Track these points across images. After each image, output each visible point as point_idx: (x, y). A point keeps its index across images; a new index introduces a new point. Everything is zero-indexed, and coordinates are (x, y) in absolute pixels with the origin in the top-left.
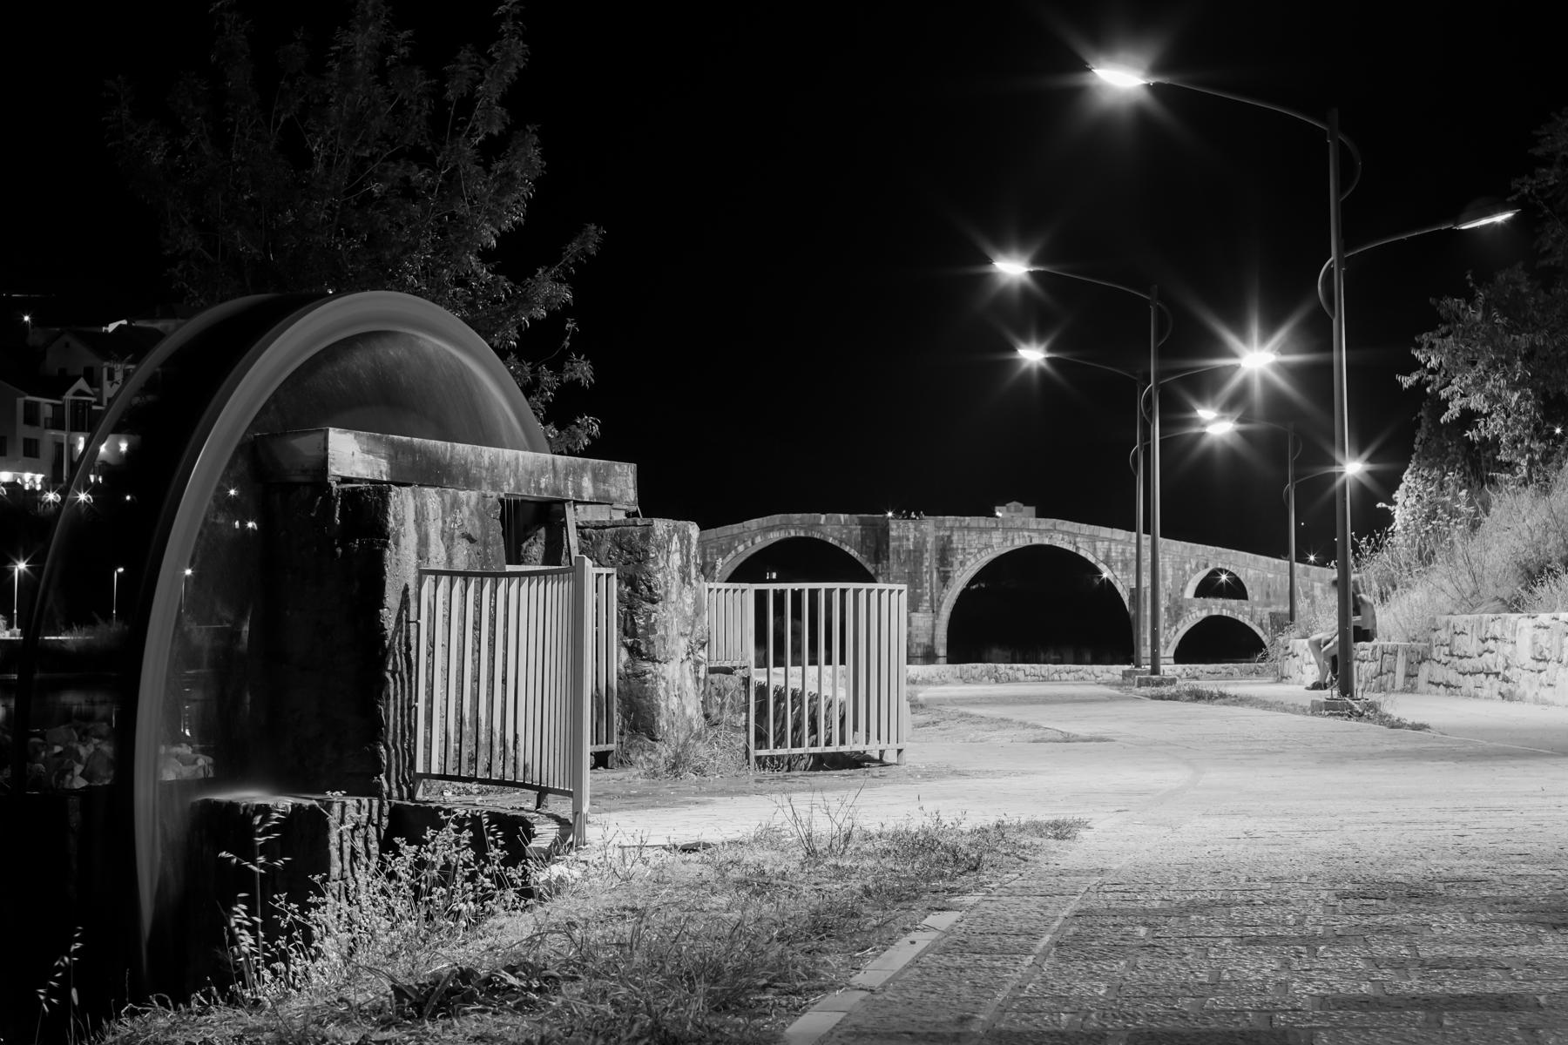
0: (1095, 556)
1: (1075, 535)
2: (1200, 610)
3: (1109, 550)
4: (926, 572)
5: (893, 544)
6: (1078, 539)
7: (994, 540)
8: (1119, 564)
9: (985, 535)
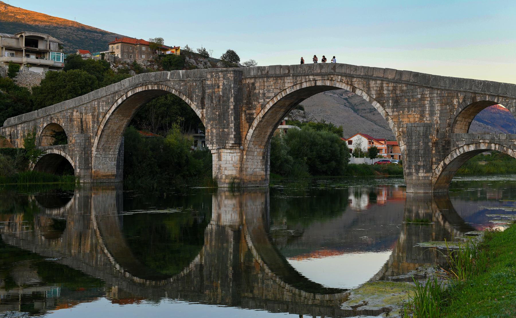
0: (368, 95)
1: (352, 77)
2: (468, 145)
3: (382, 88)
4: (232, 115)
5: (208, 91)
6: (355, 80)
7: (287, 85)
8: (391, 101)
9: (279, 81)
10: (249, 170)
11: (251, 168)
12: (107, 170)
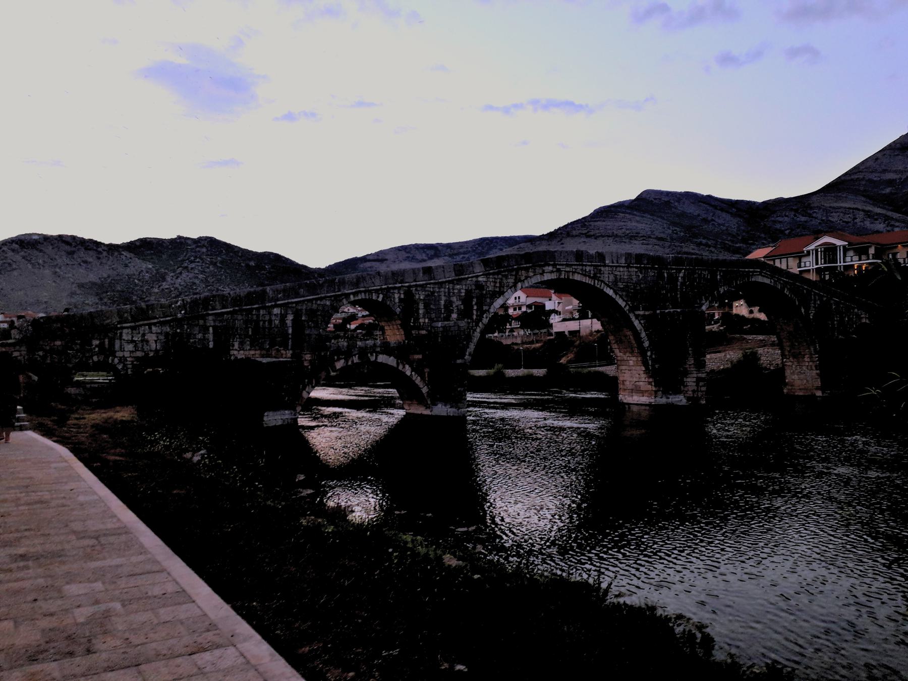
10: (627, 383)
11: (630, 381)
12: (805, 381)
